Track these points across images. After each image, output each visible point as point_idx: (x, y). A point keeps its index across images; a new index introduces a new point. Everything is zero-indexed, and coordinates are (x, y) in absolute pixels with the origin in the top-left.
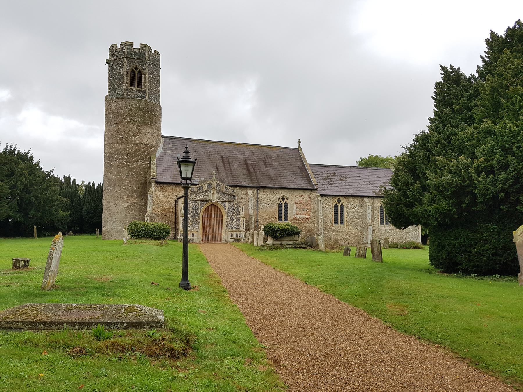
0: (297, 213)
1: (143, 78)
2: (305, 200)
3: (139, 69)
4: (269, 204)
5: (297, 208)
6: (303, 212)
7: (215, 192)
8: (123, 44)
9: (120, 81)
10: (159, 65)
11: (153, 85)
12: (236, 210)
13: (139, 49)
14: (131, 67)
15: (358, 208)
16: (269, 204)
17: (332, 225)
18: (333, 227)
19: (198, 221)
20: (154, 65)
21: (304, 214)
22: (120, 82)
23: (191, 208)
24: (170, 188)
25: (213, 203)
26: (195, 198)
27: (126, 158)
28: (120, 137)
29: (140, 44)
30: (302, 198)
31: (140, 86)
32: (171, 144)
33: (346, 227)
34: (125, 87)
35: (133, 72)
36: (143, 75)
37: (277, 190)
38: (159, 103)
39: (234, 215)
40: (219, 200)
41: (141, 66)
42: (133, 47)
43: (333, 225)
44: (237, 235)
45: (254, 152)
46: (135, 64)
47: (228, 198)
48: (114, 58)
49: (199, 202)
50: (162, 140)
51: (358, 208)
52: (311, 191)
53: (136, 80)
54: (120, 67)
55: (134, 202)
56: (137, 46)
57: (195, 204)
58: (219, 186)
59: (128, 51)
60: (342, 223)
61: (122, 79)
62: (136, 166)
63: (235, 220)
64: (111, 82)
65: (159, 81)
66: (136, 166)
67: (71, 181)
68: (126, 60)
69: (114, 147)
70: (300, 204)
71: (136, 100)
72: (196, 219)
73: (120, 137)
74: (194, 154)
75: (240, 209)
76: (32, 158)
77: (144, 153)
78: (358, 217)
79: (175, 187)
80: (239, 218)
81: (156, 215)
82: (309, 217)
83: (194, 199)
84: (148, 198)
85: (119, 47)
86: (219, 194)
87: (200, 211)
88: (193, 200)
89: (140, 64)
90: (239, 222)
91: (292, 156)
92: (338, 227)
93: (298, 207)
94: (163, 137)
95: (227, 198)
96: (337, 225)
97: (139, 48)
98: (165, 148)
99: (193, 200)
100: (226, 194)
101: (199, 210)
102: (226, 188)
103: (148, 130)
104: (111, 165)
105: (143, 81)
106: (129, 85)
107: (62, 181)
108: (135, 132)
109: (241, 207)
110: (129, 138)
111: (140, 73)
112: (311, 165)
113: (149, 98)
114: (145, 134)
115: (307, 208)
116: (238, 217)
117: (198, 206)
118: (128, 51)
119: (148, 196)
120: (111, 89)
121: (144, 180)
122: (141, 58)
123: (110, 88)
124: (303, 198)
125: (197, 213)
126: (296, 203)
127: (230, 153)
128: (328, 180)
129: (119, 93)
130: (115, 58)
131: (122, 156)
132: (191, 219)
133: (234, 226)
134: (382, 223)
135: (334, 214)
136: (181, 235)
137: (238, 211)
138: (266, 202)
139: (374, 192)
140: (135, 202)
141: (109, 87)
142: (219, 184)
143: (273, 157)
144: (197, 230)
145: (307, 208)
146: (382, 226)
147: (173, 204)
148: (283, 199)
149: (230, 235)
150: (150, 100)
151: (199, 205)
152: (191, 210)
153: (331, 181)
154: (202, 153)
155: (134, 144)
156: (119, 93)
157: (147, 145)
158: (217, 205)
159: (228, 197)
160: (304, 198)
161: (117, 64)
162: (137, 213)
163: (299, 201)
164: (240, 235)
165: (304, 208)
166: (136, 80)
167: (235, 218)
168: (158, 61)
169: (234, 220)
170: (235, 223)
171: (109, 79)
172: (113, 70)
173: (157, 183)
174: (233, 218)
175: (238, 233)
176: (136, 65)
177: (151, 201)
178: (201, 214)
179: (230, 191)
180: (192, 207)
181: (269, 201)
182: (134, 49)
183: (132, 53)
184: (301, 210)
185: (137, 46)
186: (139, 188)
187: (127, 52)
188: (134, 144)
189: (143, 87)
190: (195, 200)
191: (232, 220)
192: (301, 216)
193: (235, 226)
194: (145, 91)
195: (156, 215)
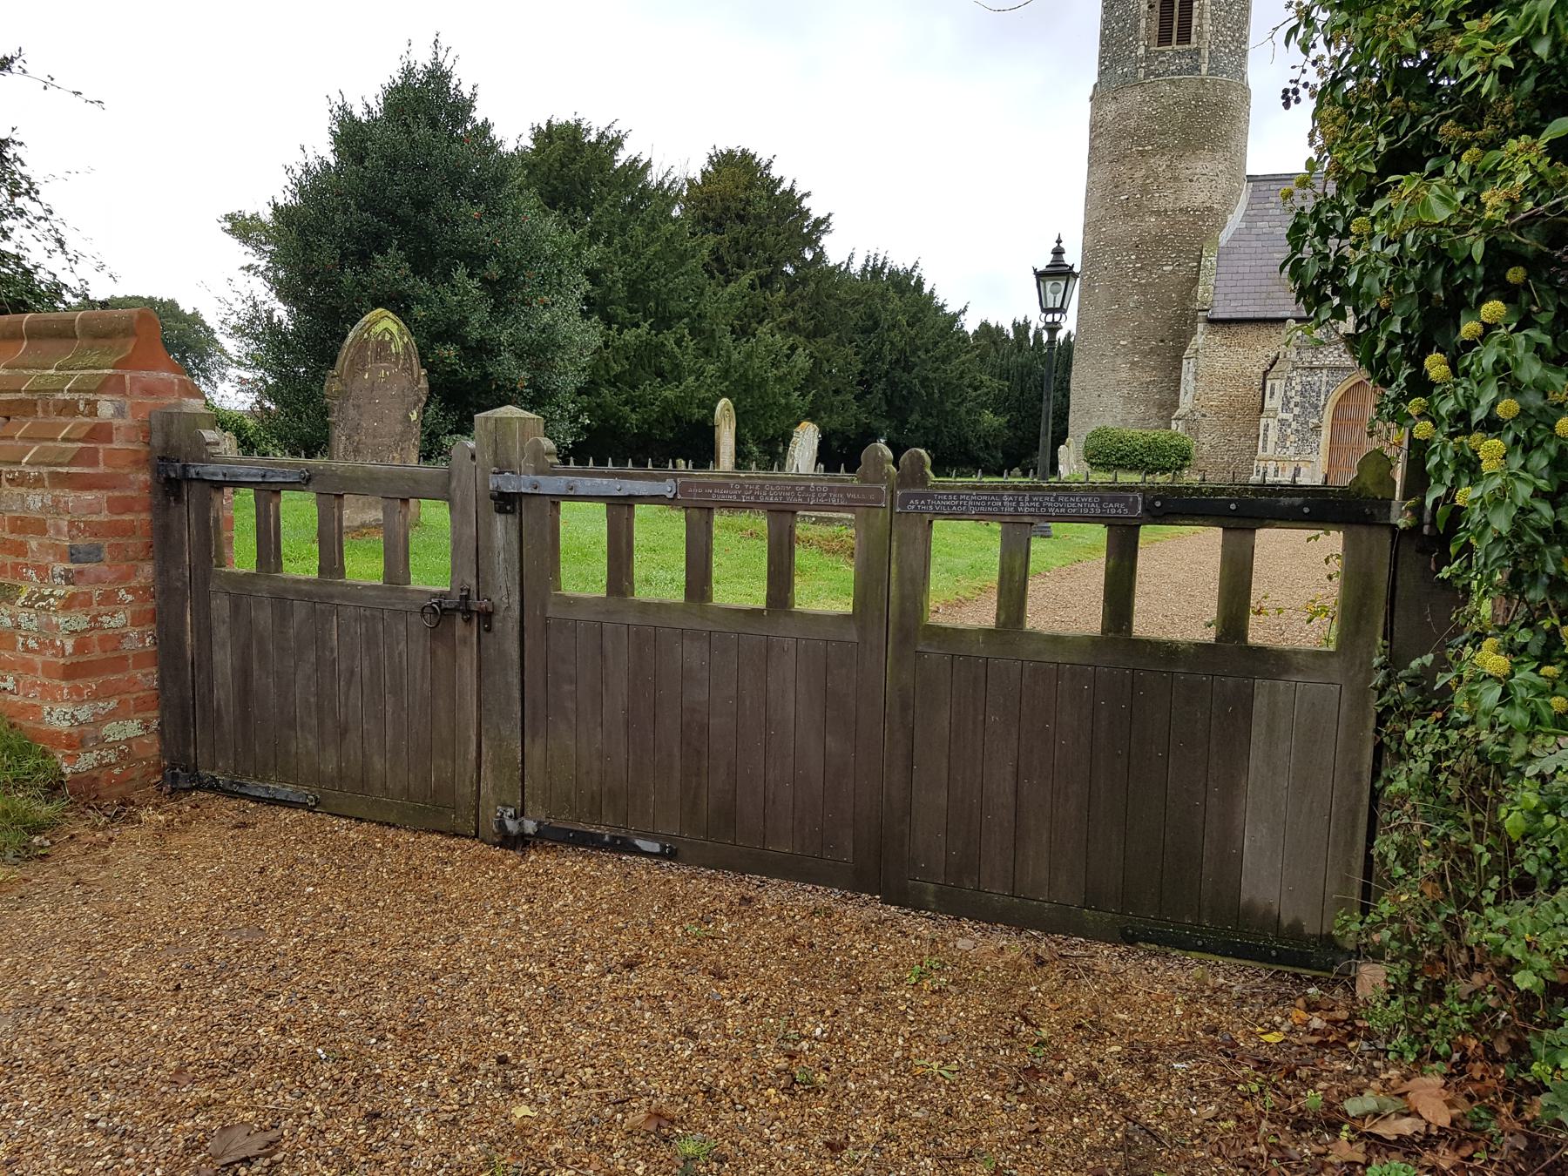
1: (1195, 13)
19: (1316, 429)
24: (1249, 334)
31: (1185, 37)
34: (1141, 51)
49: (1325, 371)
50: (1246, 191)
53: (1175, 24)
64: (1107, 42)
67: (1031, 334)
71: (1172, 82)
72: (1311, 426)
76: (920, 283)
79: (1265, 331)
81: (1204, 416)
83: (1307, 365)
84: (1184, 369)
87: (1326, 401)
88: (1304, 369)
94: (1251, 178)
98: (1252, 212)
99: (1304, 369)
101: (1323, 397)
103: (1203, 165)
104: (1095, 282)
105: (1195, 22)
107: (1008, 336)
108: (1161, 180)
113: (1209, 69)
114: (1191, 181)
119: (1185, 362)
121: (1180, 315)
125: (1317, 407)
132: (1294, 425)
141: (1100, 58)
144: (1313, 457)
147: (1257, 382)
151: (1324, 383)
152: (1297, 399)
155: (1158, 213)
162: (1154, 411)
166: (1175, 24)
171: (1102, 34)
173: (1211, 321)
177: (1190, 377)
178: (1327, 410)
186: (1162, 341)
188: (1158, 213)
189: (1194, 38)
190: (1311, 368)
194: (1198, 51)
195: (1204, 416)
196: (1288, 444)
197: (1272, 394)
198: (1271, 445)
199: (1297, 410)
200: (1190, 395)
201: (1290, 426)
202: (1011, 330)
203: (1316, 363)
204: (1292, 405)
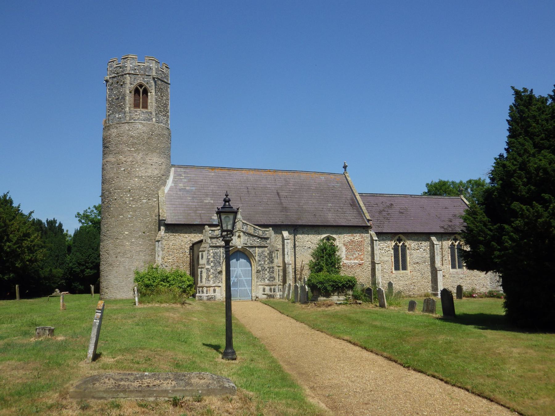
0: (347, 258)
2: (356, 241)
3: (144, 87)
4: (310, 248)
5: (346, 251)
6: (355, 256)
7: (242, 234)
9: (122, 102)
12: (268, 257)
14: (135, 84)
15: (423, 248)
16: (310, 248)
17: (392, 272)
18: (393, 274)
19: (220, 272)
21: (355, 258)
22: (122, 103)
23: (211, 256)
25: (239, 249)
26: (216, 244)
27: (128, 195)
28: (122, 169)
30: (352, 238)
31: (145, 106)
32: (183, 175)
33: (409, 274)
34: (127, 109)
35: (137, 91)
36: (149, 94)
37: (320, 229)
39: (266, 263)
40: (246, 244)
41: (147, 83)
43: (394, 272)
44: (270, 290)
45: (288, 180)
46: (140, 80)
47: (258, 242)
51: (423, 248)
52: (364, 229)
53: (141, 100)
54: (122, 85)
55: (139, 250)
57: (216, 251)
58: (246, 227)
60: (404, 268)
61: (124, 98)
62: (141, 205)
63: (268, 270)
66: (141, 205)
68: (129, 76)
69: (114, 182)
70: (350, 246)
71: (141, 123)
72: (218, 271)
73: (122, 169)
74: (212, 186)
75: (273, 255)
77: (151, 188)
78: (424, 259)
80: (273, 267)
82: (363, 263)
83: (214, 245)
89: (146, 81)
90: (273, 272)
91: (337, 185)
92: (400, 274)
93: (347, 249)
95: (257, 242)
96: (398, 272)
98: (176, 180)
100: (256, 236)
105: (149, 101)
109: (275, 253)
110: (132, 170)
111: (146, 92)
112: (361, 195)
114: (152, 165)
115: (359, 251)
116: (271, 265)
117: (219, 253)
122: (147, 74)
123: (110, 111)
124: (354, 238)
125: (219, 263)
126: (344, 245)
127: (257, 183)
128: (384, 213)
129: (120, 116)
131: (124, 193)
133: (266, 278)
134: (453, 267)
135: (393, 258)
136: (199, 292)
137: (272, 257)
138: (307, 245)
139: (443, 227)
140: (140, 251)
143: (313, 185)
145: (359, 251)
146: (454, 270)
148: (328, 239)
149: (262, 289)
150: (157, 123)
151: (222, 253)
152: (212, 259)
153: (388, 214)
154: (222, 184)
155: (138, 177)
156: (120, 116)
157: (154, 177)
159: (258, 240)
160: (356, 238)
162: (142, 264)
163: (349, 242)
164: (274, 289)
165: (355, 251)
166: (141, 100)
167: (268, 268)
169: (266, 270)
170: (268, 274)
172: (112, 89)
174: (265, 268)
175: (273, 287)
176: (141, 81)
179: (261, 233)
180: (212, 254)
181: (310, 243)
183: (136, 68)
184: (352, 253)
186: (144, 233)
187: (131, 67)
188: (138, 177)
189: (149, 107)
191: (263, 270)
192: (352, 261)
193: (268, 278)
195: (166, 266)
196: (210, 278)
197: (202, 257)
198: (204, 280)
199: (212, 264)
200: (160, 258)
201: (210, 271)
202: (46, 223)
203: (218, 244)
204: (210, 262)
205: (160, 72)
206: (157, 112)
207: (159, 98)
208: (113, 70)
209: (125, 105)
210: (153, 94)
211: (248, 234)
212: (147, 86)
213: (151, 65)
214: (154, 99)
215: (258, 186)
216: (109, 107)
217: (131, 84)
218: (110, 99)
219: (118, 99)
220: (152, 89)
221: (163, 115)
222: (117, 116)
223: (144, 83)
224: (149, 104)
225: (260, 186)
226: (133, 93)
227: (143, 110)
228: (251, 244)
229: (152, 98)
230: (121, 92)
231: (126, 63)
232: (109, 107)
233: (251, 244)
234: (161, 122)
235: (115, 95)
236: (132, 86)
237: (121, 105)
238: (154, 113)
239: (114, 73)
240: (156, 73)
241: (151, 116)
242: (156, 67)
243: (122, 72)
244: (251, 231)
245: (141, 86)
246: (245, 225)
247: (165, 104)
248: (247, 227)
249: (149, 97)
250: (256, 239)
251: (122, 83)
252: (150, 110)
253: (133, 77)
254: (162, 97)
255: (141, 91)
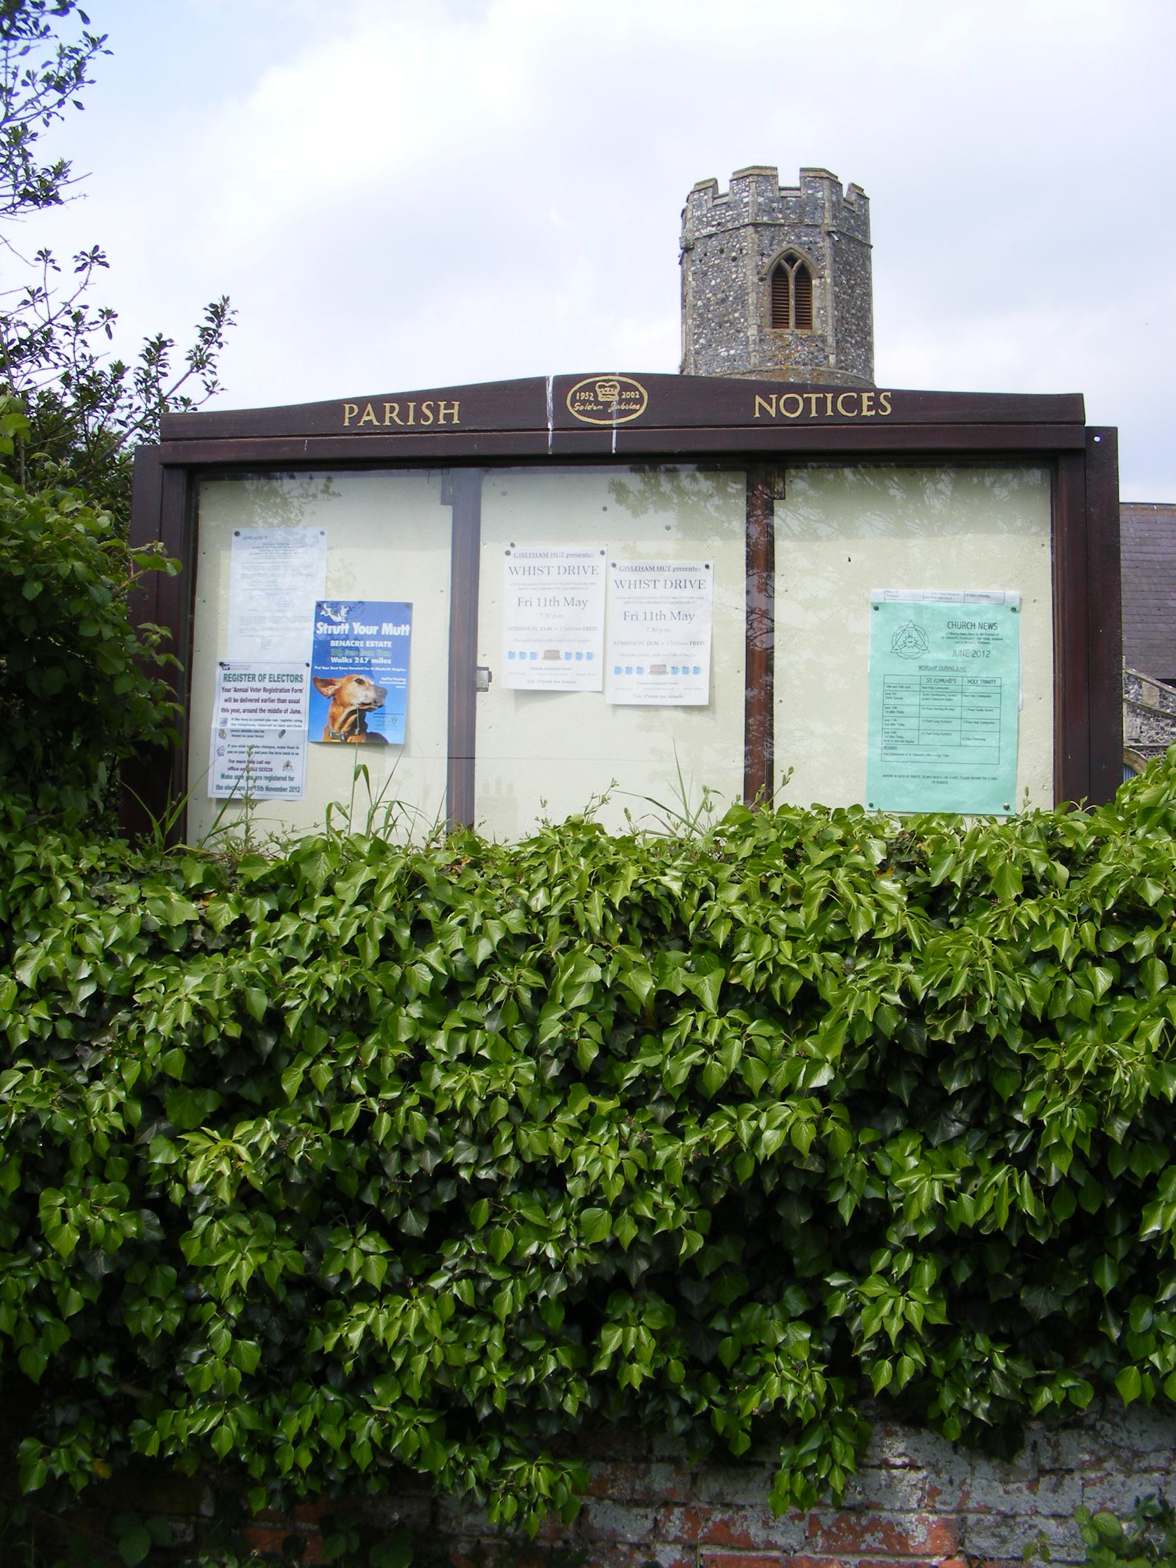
8: (740, 177)
9: (736, 311)
10: (866, 234)
11: (848, 311)
13: (798, 189)
14: (774, 255)
20: (852, 239)
22: (737, 315)
29: (802, 170)
31: (804, 321)
34: (752, 332)
35: (778, 275)
36: (815, 282)
38: (871, 376)
40: (1137, 741)
42: (777, 183)
46: (789, 242)
48: (705, 232)
54: (734, 259)
56: (789, 178)
59: (761, 200)
61: (741, 299)
64: (700, 315)
65: (868, 295)
68: (756, 232)
85: (724, 188)
86: (1139, 721)
89: (805, 243)
97: (797, 184)
100: (1167, 716)
102: (1163, 695)
105: (816, 304)
106: (768, 320)
111: (804, 276)
113: (839, 361)
118: (761, 200)
120: (702, 341)
122: (807, 221)
123: (700, 338)
127: (1145, 549)
129: (732, 352)
130: (714, 229)
142: (1137, 678)
150: (841, 368)
156: (732, 352)
158: (1130, 763)
161: (722, 251)
168: (863, 223)
176: (791, 245)
182: (781, 189)
183: (775, 205)
185: (789, 178)
187: (760, 204)
189: (816, 322)
205: (845, 214)
206: (840, 336)
207: (844, 293)
208: (705, 216)
209: (746, 320)
210: (829, 280)
211: (1142, 708)
212: (809, 257)
213: (819, 195)
214: (830, 297)
215: (1148, 557)
216: (698, 326)
217: (763, 255)
218: (700, 303)
219: (724, 301)
220: (823, 268)
221: (857, 342)
222: (724, 354)
223: (800, 250)
224: (814, 312)
225: (1154, 557)
226: (769, 282)
227: (799, 332)
228: (1153, 741)
229: (822, 297)
230: (734, 280)
231: (745, 194)
232: (698, 326)
233: (1153, 741)
234: (853, 367)
235: (714, 290)
236: (766, 260)
237: (736, 319)
238: (831, 340)
239: (709, 224)
240: (834, 217)
241: (823, 350)
242: (834, 198)
243: (734, 220)
244: (1153, 701)
245: (791, 259)
246: (1134, 683)
247: (861, 309)
248: (1141, 687)
249: (816, 293)
250: (1167, 725)
251: (734, 254)
252: (820, 332)
253: (767, 233)
254: (852, 287)
255: (792, 273)
